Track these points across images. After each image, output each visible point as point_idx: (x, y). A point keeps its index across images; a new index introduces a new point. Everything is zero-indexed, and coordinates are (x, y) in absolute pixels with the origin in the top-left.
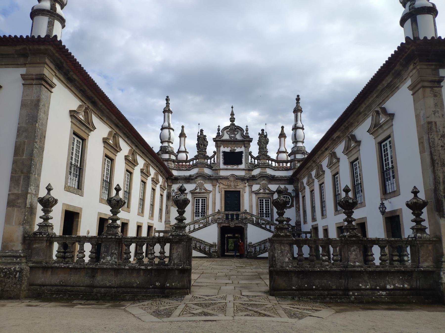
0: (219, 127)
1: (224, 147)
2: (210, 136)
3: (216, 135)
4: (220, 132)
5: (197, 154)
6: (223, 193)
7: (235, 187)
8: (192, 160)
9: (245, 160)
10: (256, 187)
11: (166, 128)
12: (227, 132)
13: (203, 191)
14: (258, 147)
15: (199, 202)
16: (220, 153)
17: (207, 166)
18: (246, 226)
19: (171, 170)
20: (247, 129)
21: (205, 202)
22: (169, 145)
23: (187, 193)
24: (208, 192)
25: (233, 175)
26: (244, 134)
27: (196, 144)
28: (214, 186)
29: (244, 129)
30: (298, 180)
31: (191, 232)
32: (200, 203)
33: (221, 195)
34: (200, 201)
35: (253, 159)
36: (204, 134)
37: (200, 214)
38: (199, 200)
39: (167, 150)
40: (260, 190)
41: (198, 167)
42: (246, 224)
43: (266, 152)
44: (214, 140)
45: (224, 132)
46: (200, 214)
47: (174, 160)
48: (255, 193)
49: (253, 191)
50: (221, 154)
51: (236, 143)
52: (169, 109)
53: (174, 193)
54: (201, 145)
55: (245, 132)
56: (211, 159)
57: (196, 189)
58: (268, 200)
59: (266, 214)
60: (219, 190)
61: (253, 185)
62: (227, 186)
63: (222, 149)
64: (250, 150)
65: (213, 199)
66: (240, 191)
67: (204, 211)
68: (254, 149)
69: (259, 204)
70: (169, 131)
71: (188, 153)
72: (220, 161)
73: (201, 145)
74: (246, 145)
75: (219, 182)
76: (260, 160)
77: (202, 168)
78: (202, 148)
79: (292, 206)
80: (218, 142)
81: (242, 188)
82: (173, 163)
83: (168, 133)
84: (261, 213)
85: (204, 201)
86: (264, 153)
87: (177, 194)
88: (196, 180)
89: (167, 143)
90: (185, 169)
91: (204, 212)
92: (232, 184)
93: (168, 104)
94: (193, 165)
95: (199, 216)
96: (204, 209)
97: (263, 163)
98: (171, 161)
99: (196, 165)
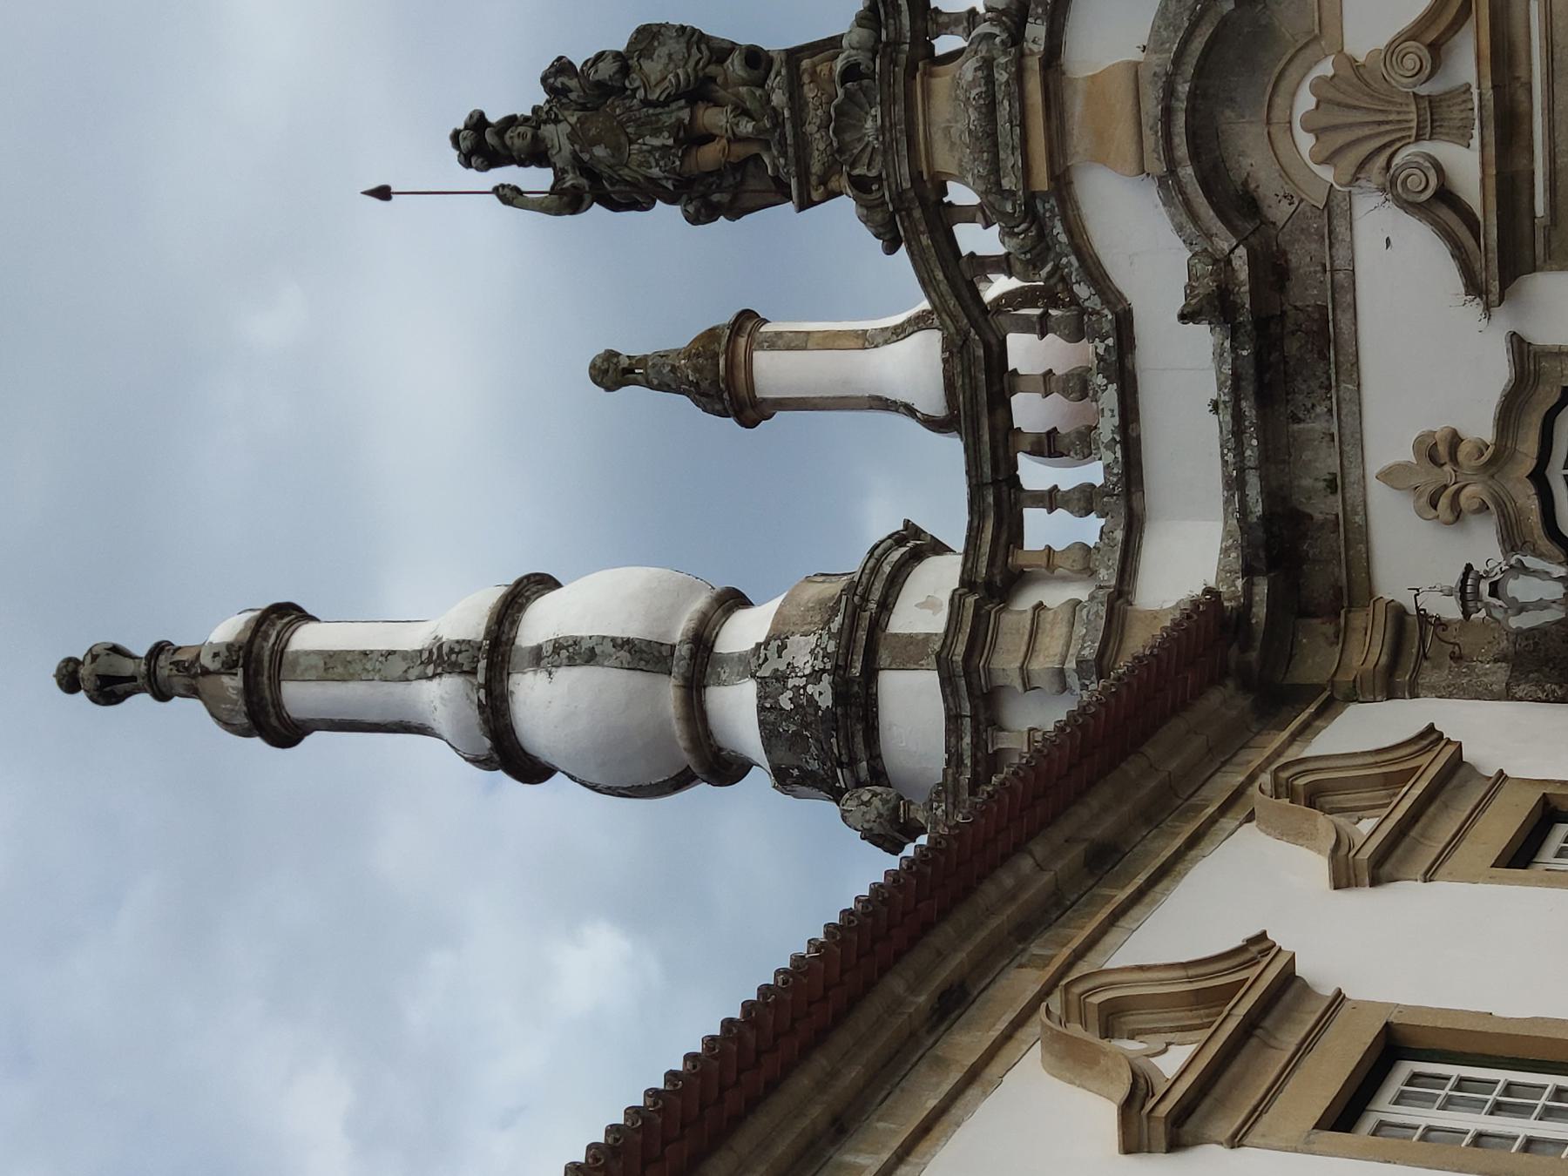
5: (843, 210)
17: (1036, 31)
19: (1138, 641)
22: (749, 664)
23: (1519, 347)
27: (694, 219)
36: (525, 97)
39: (823, 694)
41: (1062, 182)
47: (968, 582)
52: (229, 667)
53: (1520, 588)
54: (694, 138)
57: (1446, 196)
70: (537, 657)
73: (694, 138)
77: (1077, 108)
78: (747, 127)
82: (1025, 602)
83: (568, 677)
87: (1535, 518)
88: (1280, 212)
90: (1110, 398)
93: (164, 667)
94: (1034, 265)
99: (1030, 213)
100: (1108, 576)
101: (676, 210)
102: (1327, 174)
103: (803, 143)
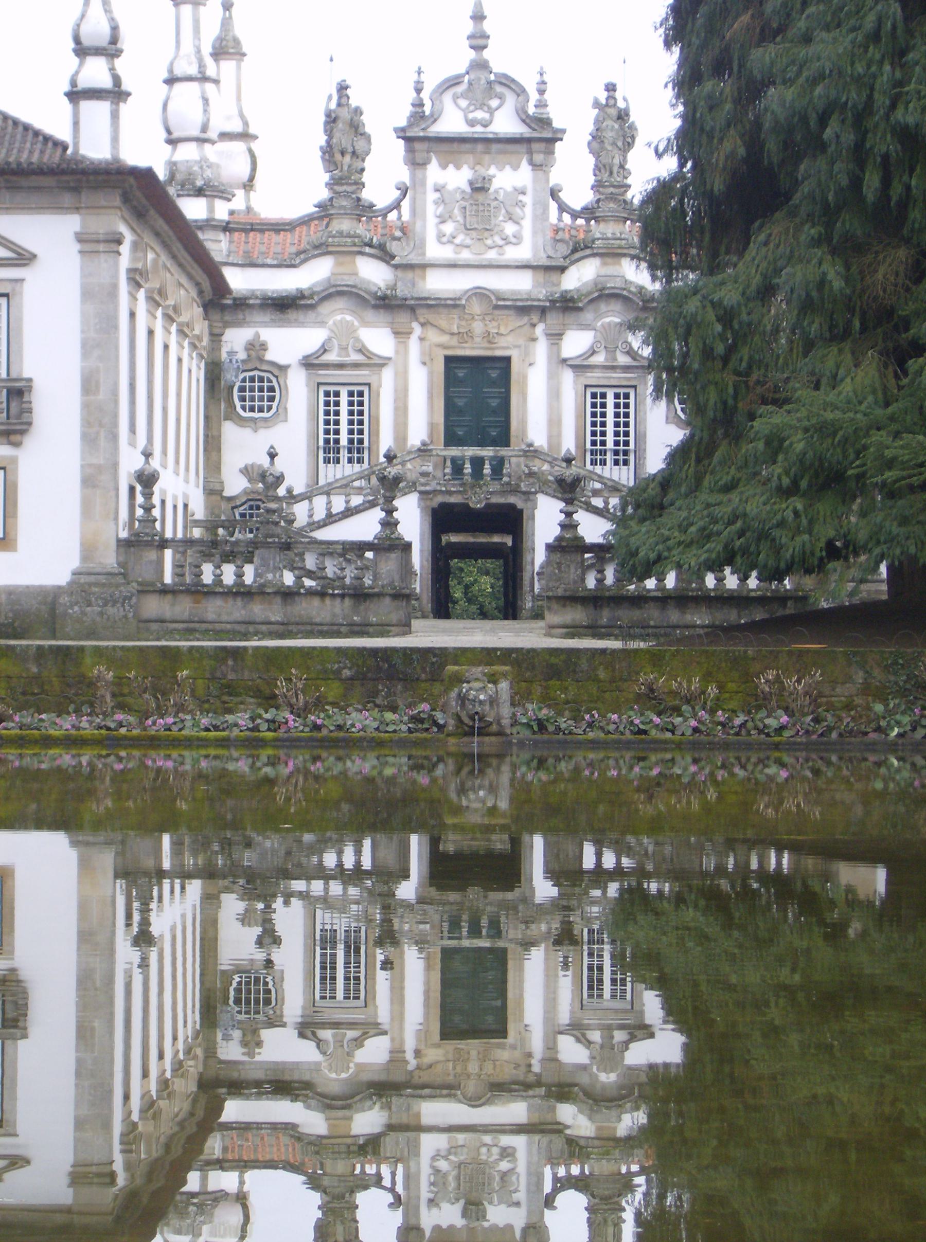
0: (419, 72)
1: (444, 166)
3: (408, 110)
4: (425, 95)
5: (324, 194)
7: (490, 342)
8: (306, 221)
9: (534, 226)
11: (190, 79)
12: (455, 98)
13: (355, 357)
14: (591, 161)
15: (337, 404)
16: (425, 193)
17: (367, 250)
18: (529, 503)
20: (543, 87)
21: (361, 404)
25: (480, 294)
26: (531, 110)
27: (321, 148)
28: (401, 334)
31: (319, 527)
32: (344, 408)
33: (431, 374)
34: (344, 399)
35: (567, 218)
36: (353, 103)
37: (344, 455)
38: (337, 394)
39: (199, 183)
40: (592, 354)
42: (528, 496)
43: (622, 186)
44: (402, 133)
45: (441, 102)
46: (344, 455)
48: (575, 368)
49: (565, 361)
50: (432, 196)
51: (495, 147)
54: (343, 153)
55: (534, 97)
56: (385, 216)
57: (325, 351)
58: (627, 396)
59: (616, 453)
60: (423, 353)
61: (561, 335)
62: (455, 338)
63: (435, 173)
64: (556, 176)
65: (396, 391)
66: (507, 360)
67: (361, 441)
69: (589, 410)
71: (255, 137)
72: (424, 226)
73: (343, 153)
74: (539, 158)
75: (422, 320)
76: (597, 219)
77: (348, 258)
78: (345, 168)
80: (418, 146)
81: (519, 347)
85: (357, 398)
86: (612, 190)
89: (193, 146)
90: (275, 262)
91: (356, 449)
92: (478, 327)
95: (338, 462)
96: (361, 432)
97: (609, 235)
98: (215, 228)
99: (321, 244)
100: (231, 260)
101: (323, 143)
102: (331, 322)
103: (342, 184)
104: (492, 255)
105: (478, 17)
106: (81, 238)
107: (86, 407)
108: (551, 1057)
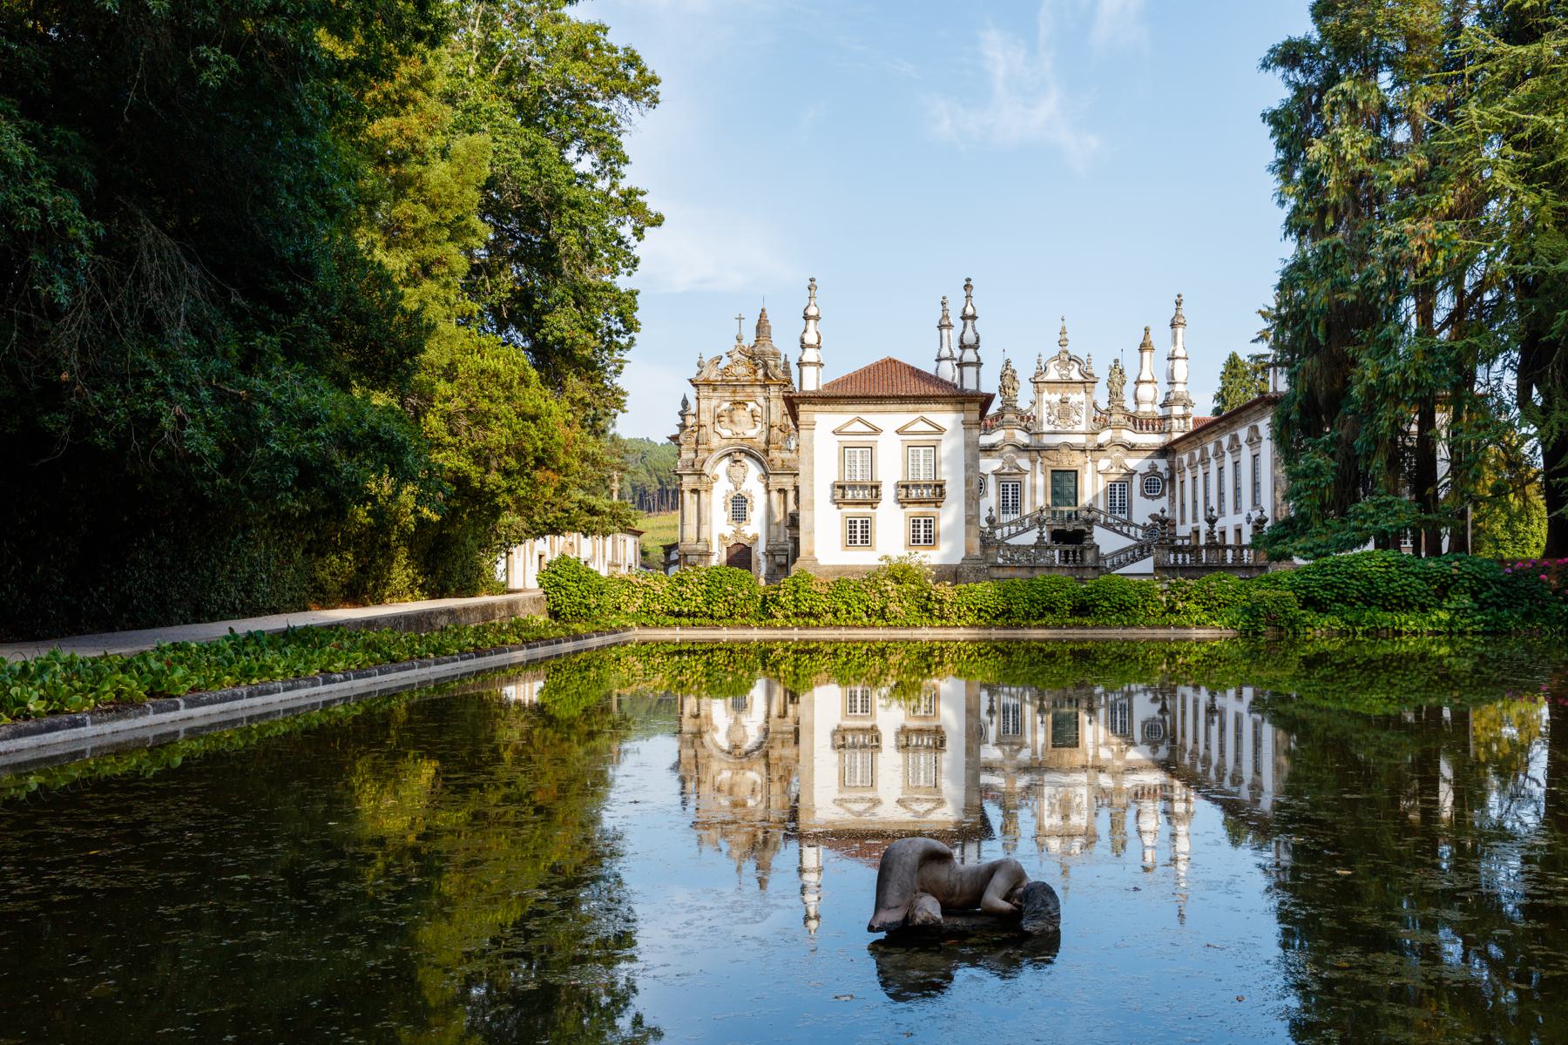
2: (1025, 372)
6: (1049, 473)
10: (1104, 464)
11: (946, 359)
13: (1015, 471)
24: (1022, 472)
28: (1033, 462)
29: (1085, 359)
30: (1175, 452)
36: (1013, 366)
50: (1045, 405)
63: (1046, 396)
68: (1101, 396)
79: (1163, 494)
84: (1112, 507)
85: (1015, 488)
91: (1016, 507)
104: (1069, 429)
105: (1063, 332)
106: (963, 423)
107: (966, 492)
108: (1096, 756)
